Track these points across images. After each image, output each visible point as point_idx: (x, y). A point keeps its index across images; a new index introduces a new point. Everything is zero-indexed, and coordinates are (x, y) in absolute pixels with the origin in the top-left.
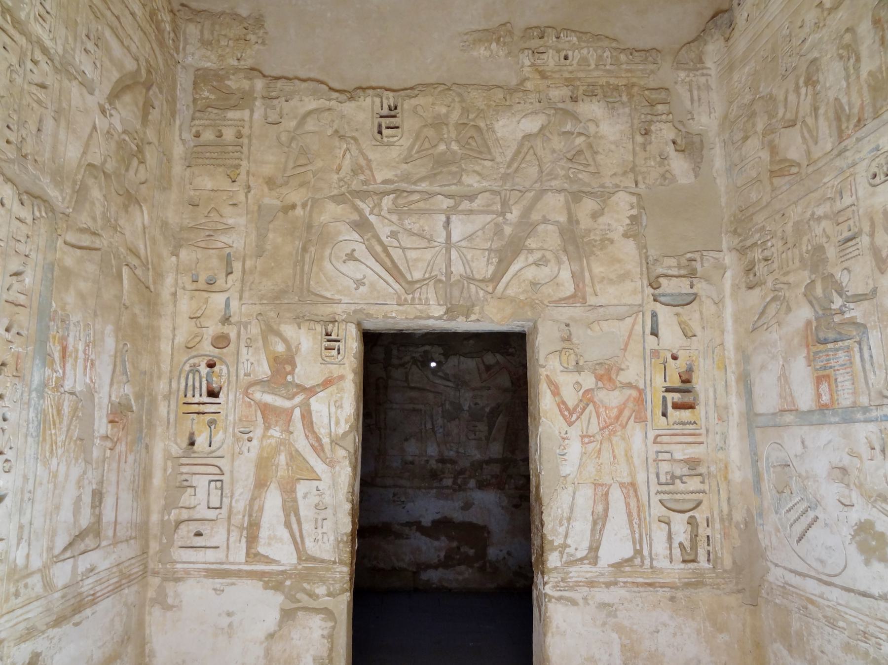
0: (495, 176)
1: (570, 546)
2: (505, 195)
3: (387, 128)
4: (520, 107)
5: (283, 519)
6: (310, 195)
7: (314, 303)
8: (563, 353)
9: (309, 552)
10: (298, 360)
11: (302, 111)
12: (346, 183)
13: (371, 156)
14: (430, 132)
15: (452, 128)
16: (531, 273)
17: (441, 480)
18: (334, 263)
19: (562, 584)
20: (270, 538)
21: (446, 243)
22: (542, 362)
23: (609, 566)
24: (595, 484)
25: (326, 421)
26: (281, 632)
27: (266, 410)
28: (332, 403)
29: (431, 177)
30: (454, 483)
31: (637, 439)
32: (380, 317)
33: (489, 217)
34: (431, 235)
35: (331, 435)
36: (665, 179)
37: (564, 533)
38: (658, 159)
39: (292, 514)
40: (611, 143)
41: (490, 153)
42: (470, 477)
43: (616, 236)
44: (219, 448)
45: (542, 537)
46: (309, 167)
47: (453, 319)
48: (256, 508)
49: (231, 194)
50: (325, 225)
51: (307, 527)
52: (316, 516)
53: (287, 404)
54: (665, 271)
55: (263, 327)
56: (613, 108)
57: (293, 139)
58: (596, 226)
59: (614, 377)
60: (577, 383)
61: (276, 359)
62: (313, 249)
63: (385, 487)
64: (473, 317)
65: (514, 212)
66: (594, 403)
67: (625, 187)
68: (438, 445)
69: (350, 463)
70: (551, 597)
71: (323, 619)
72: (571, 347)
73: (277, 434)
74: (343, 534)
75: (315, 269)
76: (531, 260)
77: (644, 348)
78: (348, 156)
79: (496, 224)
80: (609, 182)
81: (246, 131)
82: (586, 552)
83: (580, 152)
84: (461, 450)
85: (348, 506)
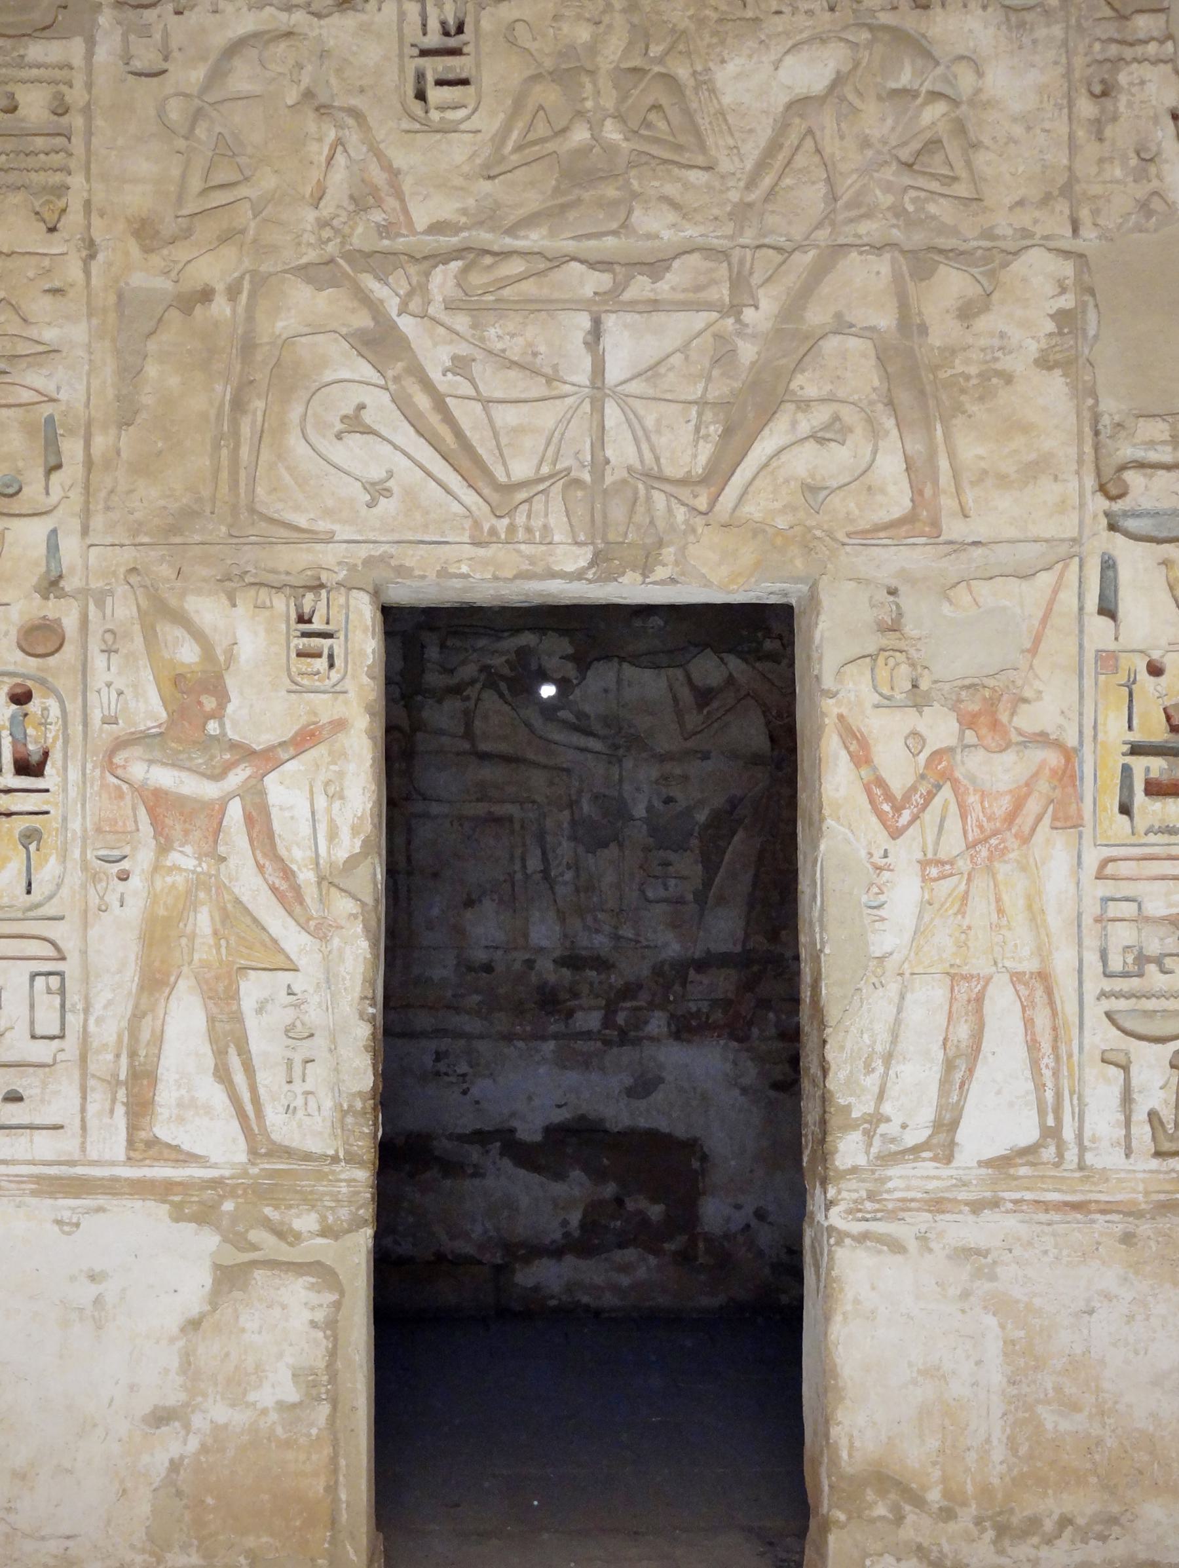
0: (716, 211)
1: (888, 1120)
2: (742, 262)
3: (440, 83)
4: (778, 24)
5: (210, 1062)
6: (247, 264)
7: (267, 543)
8: (881, 661)
9: (273, 1136)
10: (231, 683)
11: (219, 40)
12: (337, 231)
13: (399, 159)
14: (549, 95)
15: (604, 83)
16: (804, 462)
17: (570, 1014)
18: (313, 440)
19: (869, 1205)
20: (180, 1105)
21: (593, 386)
22: (828, 682)
23: (981, 1164)
24: (953, 977)
25: (305, 829)
26: (217, 1315)
27: (158, 803)
28: (319, 788)
29: (552, 215)
30: (608, 1022)
31: (1058, 869)
32: (432, 575)
33: (700, 320)
34: (555, 367)
35: (317, 864)
36: (1149, 213)
37: (876, 1090)
38: (1134, 161)
39: (232, 1051)
40: (1015, 120)
41: (703, 148)
42: (652, 1006)
43: (1017, 364)
44: (50, 897)
45: (825, 1099)
46: (243, 191)
47: (610, 577)
48: (145, 1035)
49: (46, 262)
50: (288, 342)
51: (269, 1079)
52: (289, 1054)
53: (210, 790)
54: (1140, 454)
55: (144, 603)
56: (1022, 25)
57: (198, 115)
58: (970, 341)
59: (1004, 717)
60: (915, 734)
61: (178, 680)
62: (259, 404)
64: (660, 573)
65: (764, 303)
66: (955, 783)
67: (1046, 238)
68: (562, 918)
69: (366, 928)
70: (842, 1236)
71: (311, 1288)
72: (902, 645)
73: (189, 863)
74: (354, 1095)
75: (265, 455)
76: (804, 428)
77: (1081, 646)
78: (340, 159)
79: (716, 336)
80: (1004, 224)
81: (76, 95)
82: (929, 1132)
83: (933, 145)
84: (627, 932)
85: (362, 1032)
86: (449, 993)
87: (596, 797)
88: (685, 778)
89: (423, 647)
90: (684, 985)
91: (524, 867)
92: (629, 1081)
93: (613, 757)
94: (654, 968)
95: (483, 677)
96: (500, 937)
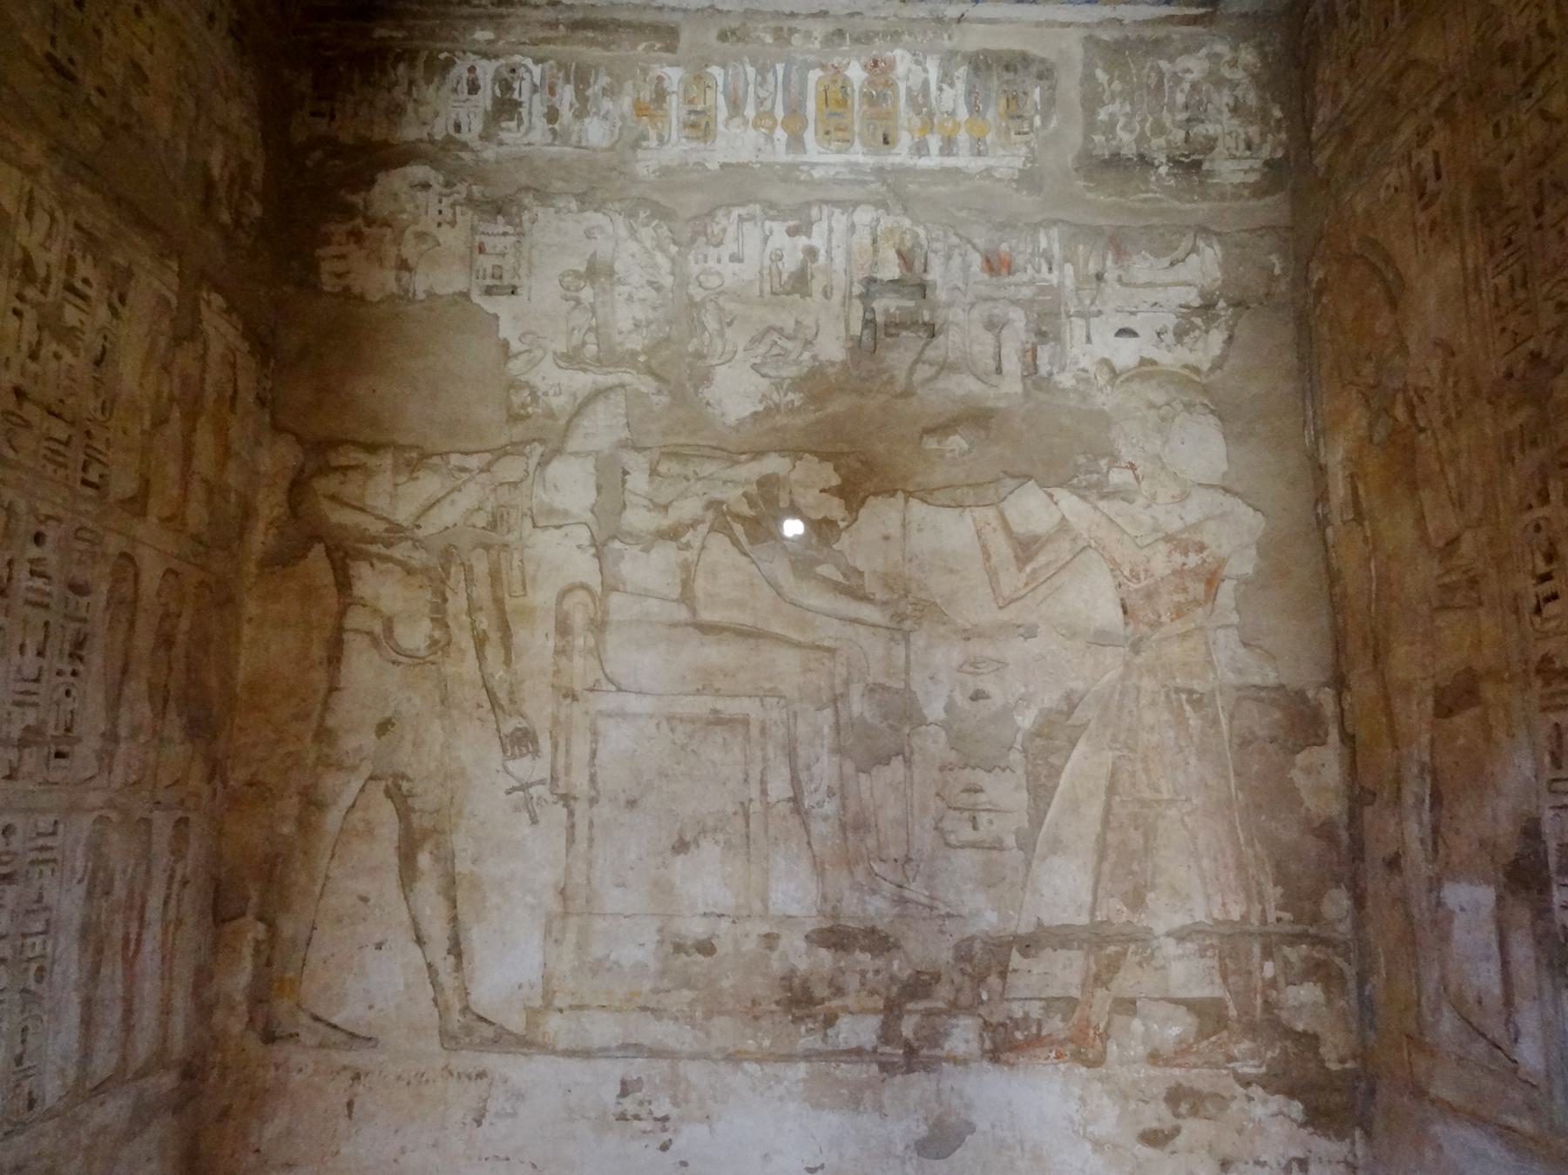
17: (830, 1020)
30: (888, 1034)
42: (955, 1008)
63: (587, 1054)
68: (818, 867)
84: (916, 891)
86: (647, 985)
87: (871, 690)
88: (1002, 664)
89: (625, 473)
90: (1003, 975)
91: (764, 792)
92: (922, 1131)
93: (899, 628)
94: (957, 947)
95: (710, 515)
96: (725, 899)
